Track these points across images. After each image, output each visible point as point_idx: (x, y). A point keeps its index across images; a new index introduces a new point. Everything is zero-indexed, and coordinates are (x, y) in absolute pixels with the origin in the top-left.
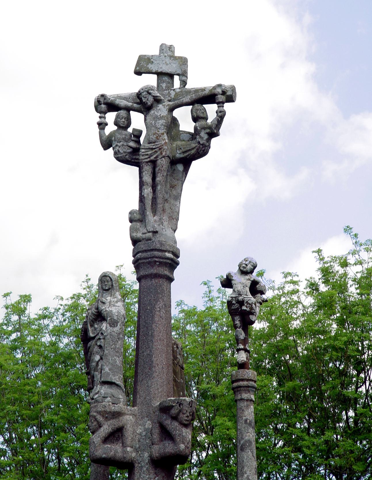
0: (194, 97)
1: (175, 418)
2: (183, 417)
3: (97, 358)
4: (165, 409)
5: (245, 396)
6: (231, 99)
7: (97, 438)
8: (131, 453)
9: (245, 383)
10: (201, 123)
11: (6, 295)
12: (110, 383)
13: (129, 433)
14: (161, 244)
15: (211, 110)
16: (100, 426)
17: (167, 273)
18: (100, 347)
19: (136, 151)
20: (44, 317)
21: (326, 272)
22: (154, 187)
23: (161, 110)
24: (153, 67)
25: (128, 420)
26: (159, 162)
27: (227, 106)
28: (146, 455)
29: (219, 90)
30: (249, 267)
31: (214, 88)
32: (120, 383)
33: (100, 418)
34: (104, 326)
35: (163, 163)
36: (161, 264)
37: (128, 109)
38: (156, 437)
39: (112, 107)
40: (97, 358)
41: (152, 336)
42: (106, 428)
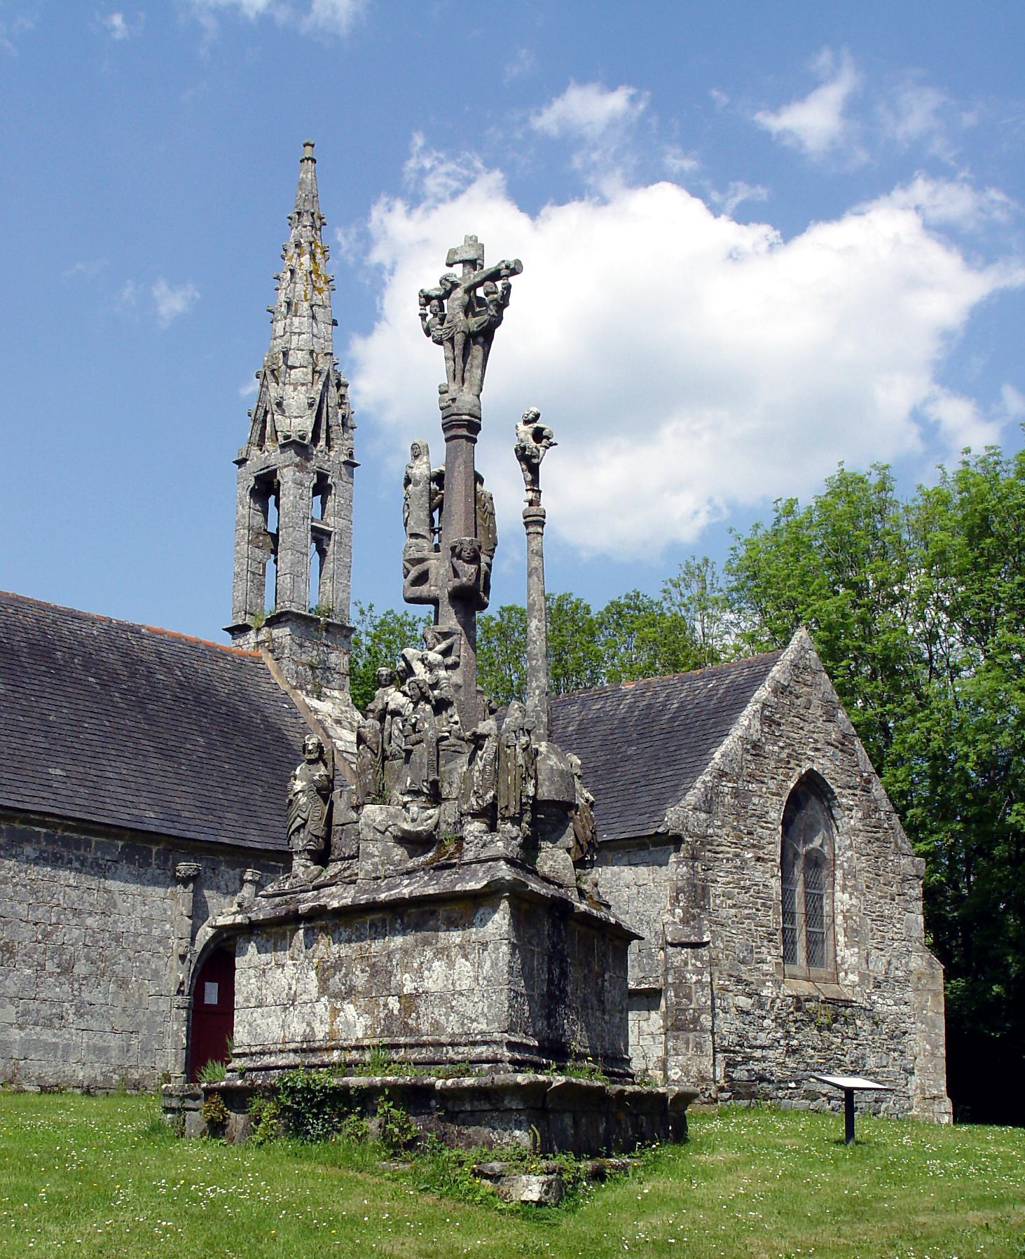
6: (514, 272)
9: (535, 518)
13: (432, 576)
14: (458, 409)
15: (499, 284)
25: (432, 564)
27: (512, 280)
30: (531, 416)
31: (499, 264)
36: (459, 426)
41: (452, 489)
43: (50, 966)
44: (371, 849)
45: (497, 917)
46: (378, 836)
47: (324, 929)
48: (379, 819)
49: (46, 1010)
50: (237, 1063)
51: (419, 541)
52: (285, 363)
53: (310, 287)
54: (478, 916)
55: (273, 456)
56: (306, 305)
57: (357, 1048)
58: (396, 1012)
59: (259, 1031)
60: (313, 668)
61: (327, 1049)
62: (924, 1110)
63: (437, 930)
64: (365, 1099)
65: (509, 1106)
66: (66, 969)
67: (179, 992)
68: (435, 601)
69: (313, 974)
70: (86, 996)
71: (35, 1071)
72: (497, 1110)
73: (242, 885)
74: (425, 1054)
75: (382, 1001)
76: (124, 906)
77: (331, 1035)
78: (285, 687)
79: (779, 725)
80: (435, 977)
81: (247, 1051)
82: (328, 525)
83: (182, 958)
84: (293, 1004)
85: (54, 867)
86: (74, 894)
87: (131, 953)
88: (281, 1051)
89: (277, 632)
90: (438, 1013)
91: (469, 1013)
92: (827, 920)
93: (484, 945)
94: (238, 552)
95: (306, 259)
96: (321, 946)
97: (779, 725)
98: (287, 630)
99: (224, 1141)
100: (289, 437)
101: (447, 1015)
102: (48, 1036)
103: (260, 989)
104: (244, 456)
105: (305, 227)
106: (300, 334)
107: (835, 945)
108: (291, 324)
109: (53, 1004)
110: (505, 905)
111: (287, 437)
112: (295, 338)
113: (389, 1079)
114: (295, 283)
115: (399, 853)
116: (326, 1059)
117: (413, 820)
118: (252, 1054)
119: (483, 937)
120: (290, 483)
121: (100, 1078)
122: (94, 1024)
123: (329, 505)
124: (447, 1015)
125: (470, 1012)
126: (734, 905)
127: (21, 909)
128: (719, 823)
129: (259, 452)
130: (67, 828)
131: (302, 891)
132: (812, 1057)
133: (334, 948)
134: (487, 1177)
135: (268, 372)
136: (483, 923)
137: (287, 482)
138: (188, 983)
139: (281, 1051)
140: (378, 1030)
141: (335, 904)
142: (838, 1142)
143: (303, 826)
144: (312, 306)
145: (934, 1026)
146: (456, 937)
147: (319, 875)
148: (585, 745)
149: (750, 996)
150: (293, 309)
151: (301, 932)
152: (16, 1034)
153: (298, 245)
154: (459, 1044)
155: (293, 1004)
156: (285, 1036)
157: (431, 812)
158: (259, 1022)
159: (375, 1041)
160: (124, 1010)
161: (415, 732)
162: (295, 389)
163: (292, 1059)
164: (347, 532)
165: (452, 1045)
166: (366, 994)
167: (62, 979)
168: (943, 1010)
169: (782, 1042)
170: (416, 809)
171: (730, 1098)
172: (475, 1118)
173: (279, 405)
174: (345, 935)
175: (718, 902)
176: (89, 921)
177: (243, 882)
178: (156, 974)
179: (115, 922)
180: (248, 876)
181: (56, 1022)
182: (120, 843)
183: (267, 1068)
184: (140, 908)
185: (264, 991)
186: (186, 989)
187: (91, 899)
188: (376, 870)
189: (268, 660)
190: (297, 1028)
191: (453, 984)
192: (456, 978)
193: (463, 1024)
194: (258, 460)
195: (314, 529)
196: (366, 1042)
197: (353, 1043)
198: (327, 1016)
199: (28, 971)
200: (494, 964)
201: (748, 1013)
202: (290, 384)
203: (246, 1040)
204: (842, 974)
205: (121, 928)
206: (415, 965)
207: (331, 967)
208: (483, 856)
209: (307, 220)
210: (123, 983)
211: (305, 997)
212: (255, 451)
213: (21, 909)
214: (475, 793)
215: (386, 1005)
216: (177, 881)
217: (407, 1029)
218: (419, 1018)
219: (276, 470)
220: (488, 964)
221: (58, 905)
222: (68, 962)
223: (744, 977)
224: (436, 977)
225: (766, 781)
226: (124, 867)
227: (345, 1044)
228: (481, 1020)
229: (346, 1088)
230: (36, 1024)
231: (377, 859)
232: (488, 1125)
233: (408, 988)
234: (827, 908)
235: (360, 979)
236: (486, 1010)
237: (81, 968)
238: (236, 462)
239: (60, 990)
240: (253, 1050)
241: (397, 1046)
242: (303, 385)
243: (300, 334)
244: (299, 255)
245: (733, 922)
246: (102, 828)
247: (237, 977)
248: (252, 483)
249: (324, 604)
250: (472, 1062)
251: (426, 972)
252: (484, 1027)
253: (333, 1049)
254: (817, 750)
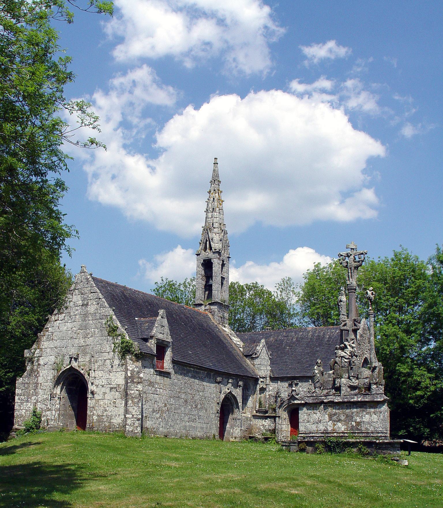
0: (359, 254)
1: (357, 322)
2: (358, 321)
3: (341, 309)
4: (355, 320)
5: (371, 316)
6: (366, 254)
7: (341, 325)
8: (348, 328)
10: (360, 259)
11: (314, 263)
12: (344, 315)
13: (347, 324)
16: (342, 323)
17: (354, 291)
18: (341, 307)
19: (347, 265)
20: (324, 268)
21: (396, 256)
22: (351, 273)
23: (352, 257)
24: (349, 247)
26: (352, 268)
28: (351, 329)
29: (364, 252)
32: (345, 314)
33: (342, 322)
34: (342, 303)
35: (353, 268)
36: (353, 290)
37: (345, 256)
38: (353, 325)
39: (341, 255)
40: (341, 309)
42: (343, 323)
44: (343, 389)
45: (384, 406)
46: (345, 386)
47: (329, 406)
48: (345, 382)
50: (301, 435)
51: (344, 316)
52: (213, 226)
53: (219, 203)
54: (379, 406)
55: (209, 254)
56: (218, 209)
57: (342, 433)
58: (354, 425)
59: (308, 428)
60: (221, 318)
61: (332, 433)
63: (367, 408)
64: (354, 445)
65: (396, 446)
67: (218, 413)
68: (348, 331)
69: (327, 416)
71: (191, 434)
72: (393, 447)
73: (228, 384)
74: (365, 435)
75: (350, 423)
77: (333, 430)
78: (216, 324)
79: (360, 345)
80: (366, 418)
81: (305, 432)
82: (223, 275)
83: (218, 403)
84: (320, 422)
85: (194, 379)
86: (198, 386)
88: (316, 433)
89: (212, 307)
90: (368, 426)
91: (377, 426)
93: (381, 412)
94: (197, 282)
95: (217, 194)
96: (329, 410)
97: (360, 345)
98: (216, 307)
99: (305, 453)
100: (216, 250)
101: (370, 427)
103: (308, 418)
104: (199, 253)
105: (216, 184)
106: (216, 218)
108: (214, 215)
110: (386, 404)
111: (215, 250)
112: (215, 219)
113: (362, 440)
114: (215, 202)
115: (349, 390)
116: (333, 435)
117: (353, 383)
118: (306, 433)
119: (380, 410)
120: (216, 264)
123: (224, 269)
124: (370, 427)
125: (377, 425)
129: (204, 252)
131: (320, 396)
133: (334, 410)
134: (396, 460)
135: (208, 229)
136: (380, 408)
137: (215, 263)
138: (219, 410)
139: (316, 433)
140: (349, 429)
141: (337, 401)
142: (406, 455)
143: (319, 381)
144: (219, 210)
146: (372, 410)
147: (322, 393)
148: (301, 346)
150: (214, 210)
151: (322, 406)
153: (214, 190)
154: (374, 433)
155: (320, 422)
156: (317, 429)
157: (357, 381)
158: (308, 426)
159: (349, 431)
161: (353, 363)
162: (216, 235)
163: (320, 435)
164: (228, 277)
165: (372, 433)
166: (345, 421)
168: (389, 421)
170: (354, 380)
172: (386, 449)
173: (212, 239)
174: (337, 408)
177: (228, 383)
179: (205, 394)
180: (230, 381)
183: (313, 437)
184: (209, 390)
185: (310, 419)
186: (219, 412)
187: (201, 388)
188: (344, 393)
189: (210, 315)
190: (322, 427)
191: (372, 420)
192: (372, 419)
193: (375, 429)
194: (205, 255)
195: (222, 277)
196: (345, 432)
197: (341, 432)
198: (332, 426)
200: (384, 417)
202: (214, 233)
203: (304, 430)
206: (360, 415)
207: (333, 414)
208: (377, 393)
209: (216, 182)
210: (206, 410)
211: (324, 421)
212: (203, 252)
214: (375, 379)
215: (351, 424)
216: (216, 382)
217: (358, 429)
218: (361, 427)
219: (211, 259)
220: (382, 416)
221: (195, 389)
222: (197, 404)
224: (366, 418)
226: (207, 379)
227: (338, 432)
228: (380, 428)
229: (349, 442)
231: (344, 391)
232: (390, 450)
233: (358, 420)
235: (343, 418)
236: (381, 426)
237: (199, 406)
238: (196, 254)
239: (195, 412)
240: (307, 432)
241: (356, 433)
242: (218, 233)
243: (216, 218)
244: (215, 193)
246: (204, 369)
247: (299, 415)
248: (202, 262)
249: (222, 298)
250: (379, 437)
251: (364, 417)
252: (381, 430)
253: (334, 433)
254: (367, 351)
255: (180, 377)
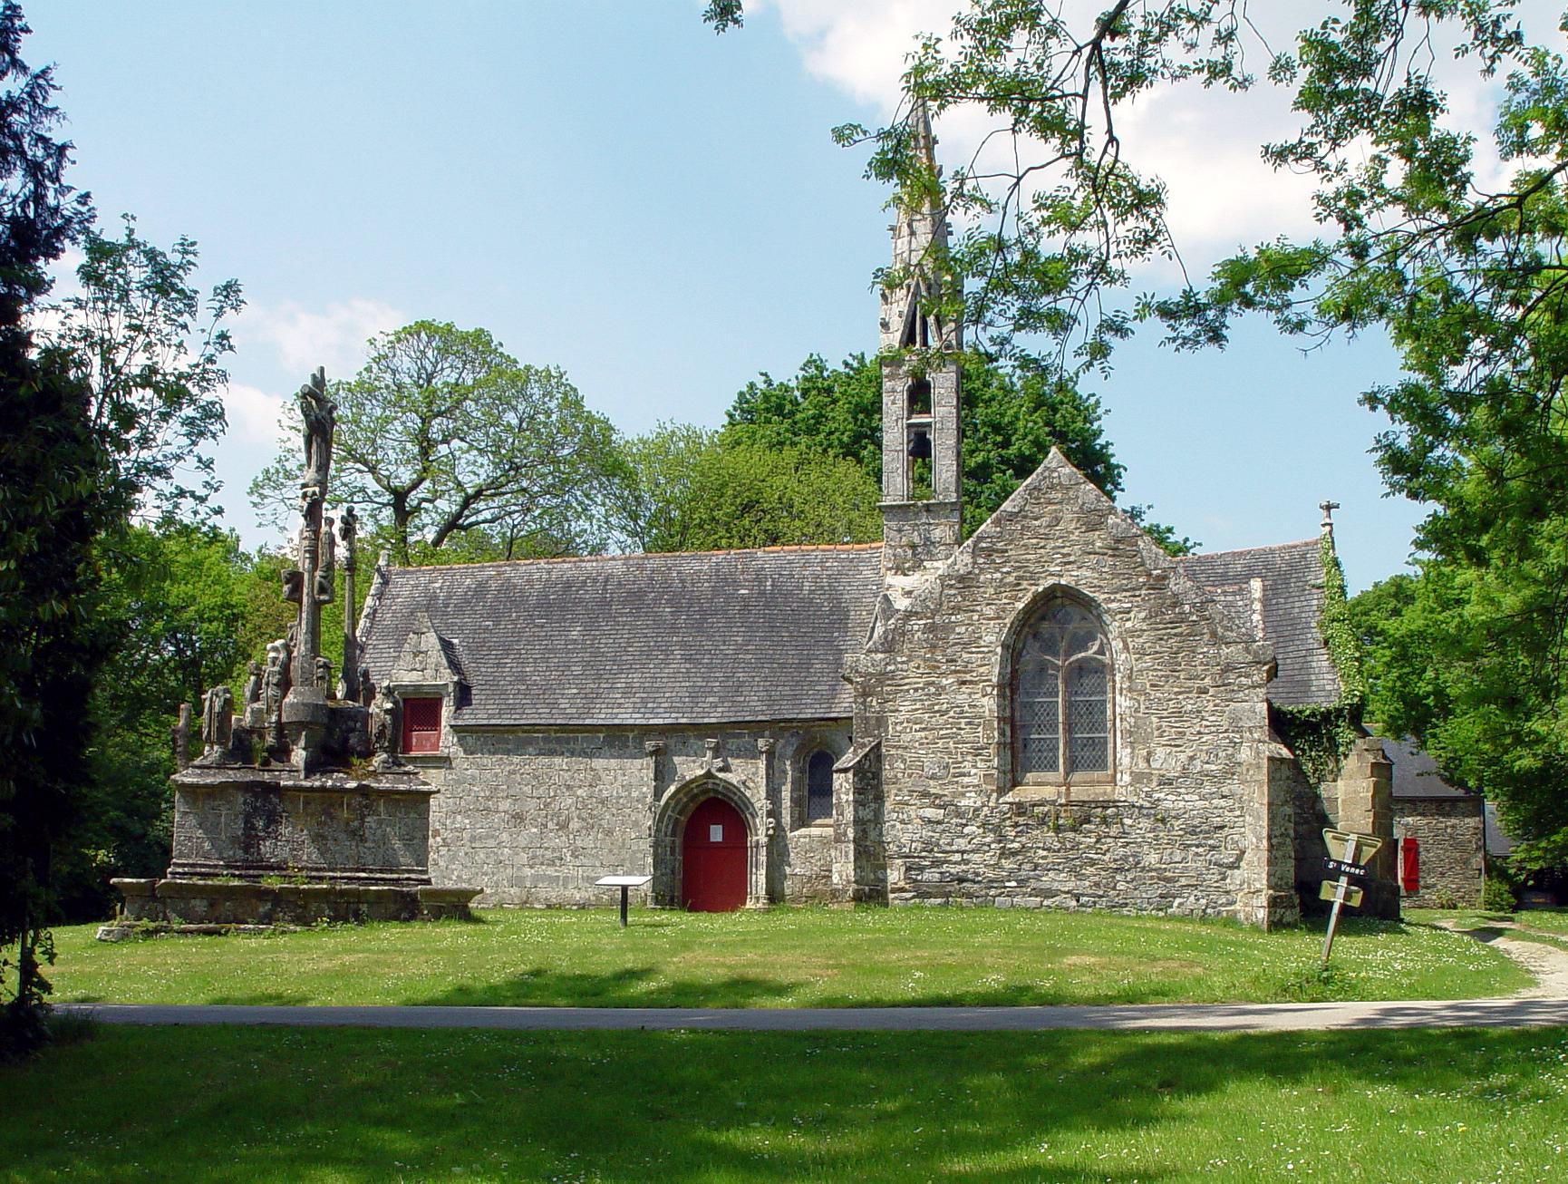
43: (550, 825)
49: (549, 854)
62: (1246, 905)
66: (563, 826)
70: (579, 843)
71: (543, 895)
76: (607, 778)
86: (566, 775)
87: (615, 811)
92: (1109, 725)
102: (550, 871)
107: (1115, 747)
109: (554, 850)
121: (593, 898)
122: (585, 861)
126: (924, 729)
127: (527, 789)
128: (904, 659)
130: (556, 732)
132: (1044, 858)
145: (1259, 818)
149: (943, 807)
152: (528, 871)
160: (611, 851)
167: (560, 833)
169: (993, 846)
171: (914, 897)
175: (899, 728)
176: (579, 792)
178: (636, 824)
181: (558, 862)
182: (601, 735)
184: (620, 778)
199: (534, 830)
201: (939, 823)
204: (1119, 776)
205: (605, 794)
210: (609, 833)
213: (527, 789)
223: (932, 791)
225: (978, 608)
230: (542, 864)
234: (1109, 712)
237: (575, 825)
245: (921, 744)
255: (487, 760)
